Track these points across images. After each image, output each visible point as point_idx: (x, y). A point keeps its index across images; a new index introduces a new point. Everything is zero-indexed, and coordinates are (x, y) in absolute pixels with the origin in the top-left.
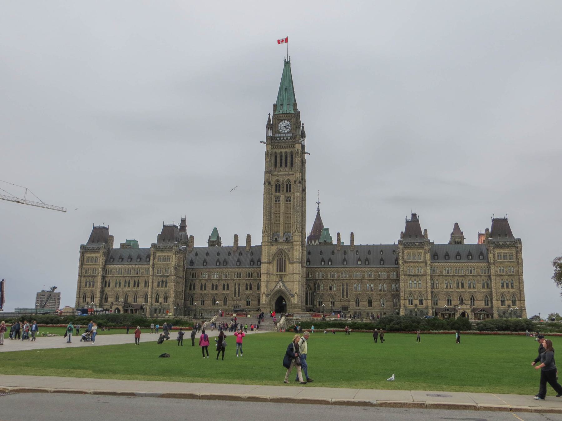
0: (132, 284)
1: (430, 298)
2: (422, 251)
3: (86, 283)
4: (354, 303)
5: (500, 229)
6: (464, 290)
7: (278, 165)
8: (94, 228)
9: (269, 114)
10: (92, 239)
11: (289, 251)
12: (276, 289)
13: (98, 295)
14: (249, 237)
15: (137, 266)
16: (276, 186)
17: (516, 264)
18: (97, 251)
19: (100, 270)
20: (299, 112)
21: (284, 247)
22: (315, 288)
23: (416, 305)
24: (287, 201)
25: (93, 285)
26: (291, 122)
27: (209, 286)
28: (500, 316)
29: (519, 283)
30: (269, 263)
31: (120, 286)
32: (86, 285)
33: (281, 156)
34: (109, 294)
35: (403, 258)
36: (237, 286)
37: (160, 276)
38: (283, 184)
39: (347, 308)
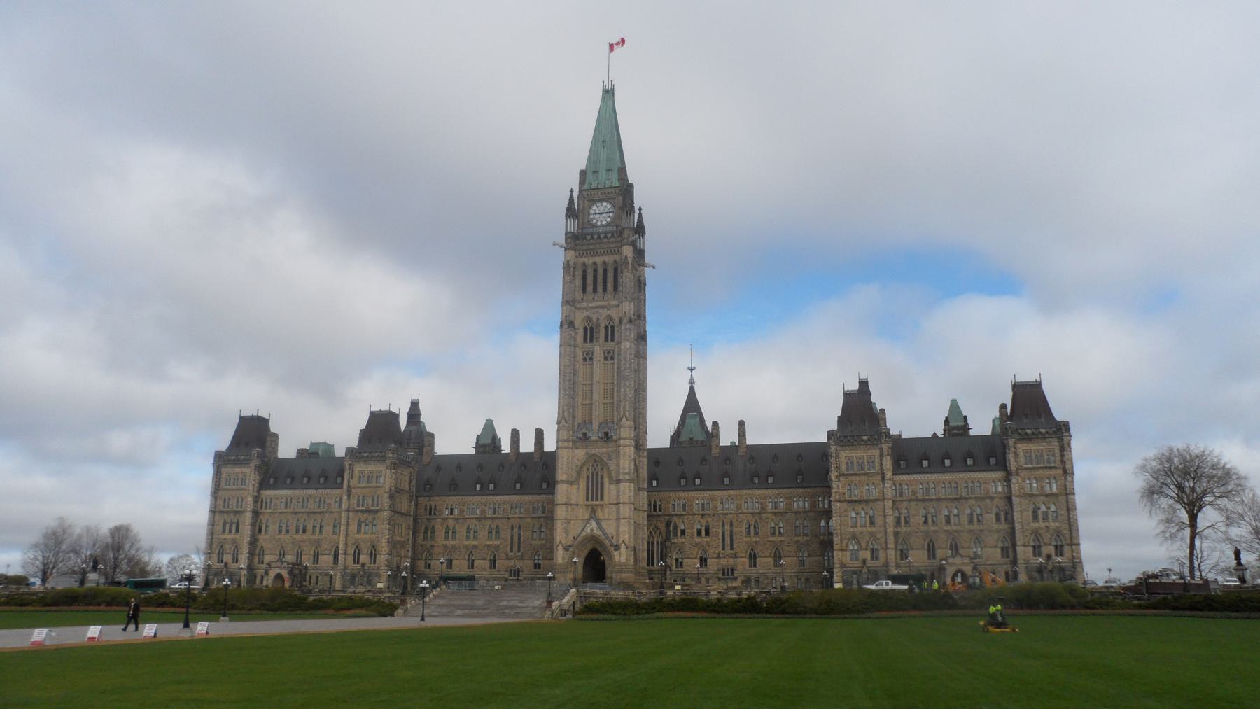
0: (309, 528)
1: (891, 545)
2: (875, 452)
3: (224, 526)
4: (747, 561)
5: (1029, 405)
6: (959, 528)
7: (590, 288)
8: (242, 418)
9: (572, 191)
11: (610, 458)
12: (584, 534)
13: (245, 549)
14: (539, 434)
15: (320, 492)
16: (585, 329)
17: (1060, 471)
18: (246, 463)
19: (250, 499)
20: (631, 186)
21: (601, 450)
22: (668, 532)
23: (864, 561)
24: (606, 359)
25: (237, 531)
26: (613, 206)
27: (462, 531)
28: (1031, 578)
29: (1068, 510)
30: (571, 483)
31: (287, 532)
32: (224, 531)
33: (595, 271)
35: (838, 468)
36: (516, 530)
38: (598, 325)
39: (732, 570)
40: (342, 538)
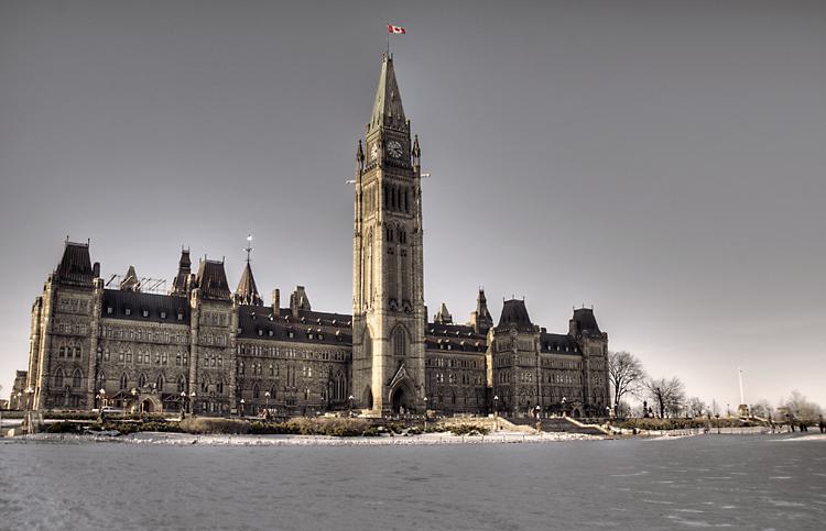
5: (584, 321)
15: (163, 325)
17: (602, 359)
19: (94, 324)
33: (393, 190)
36: (291, 369)
40: (192, 369)
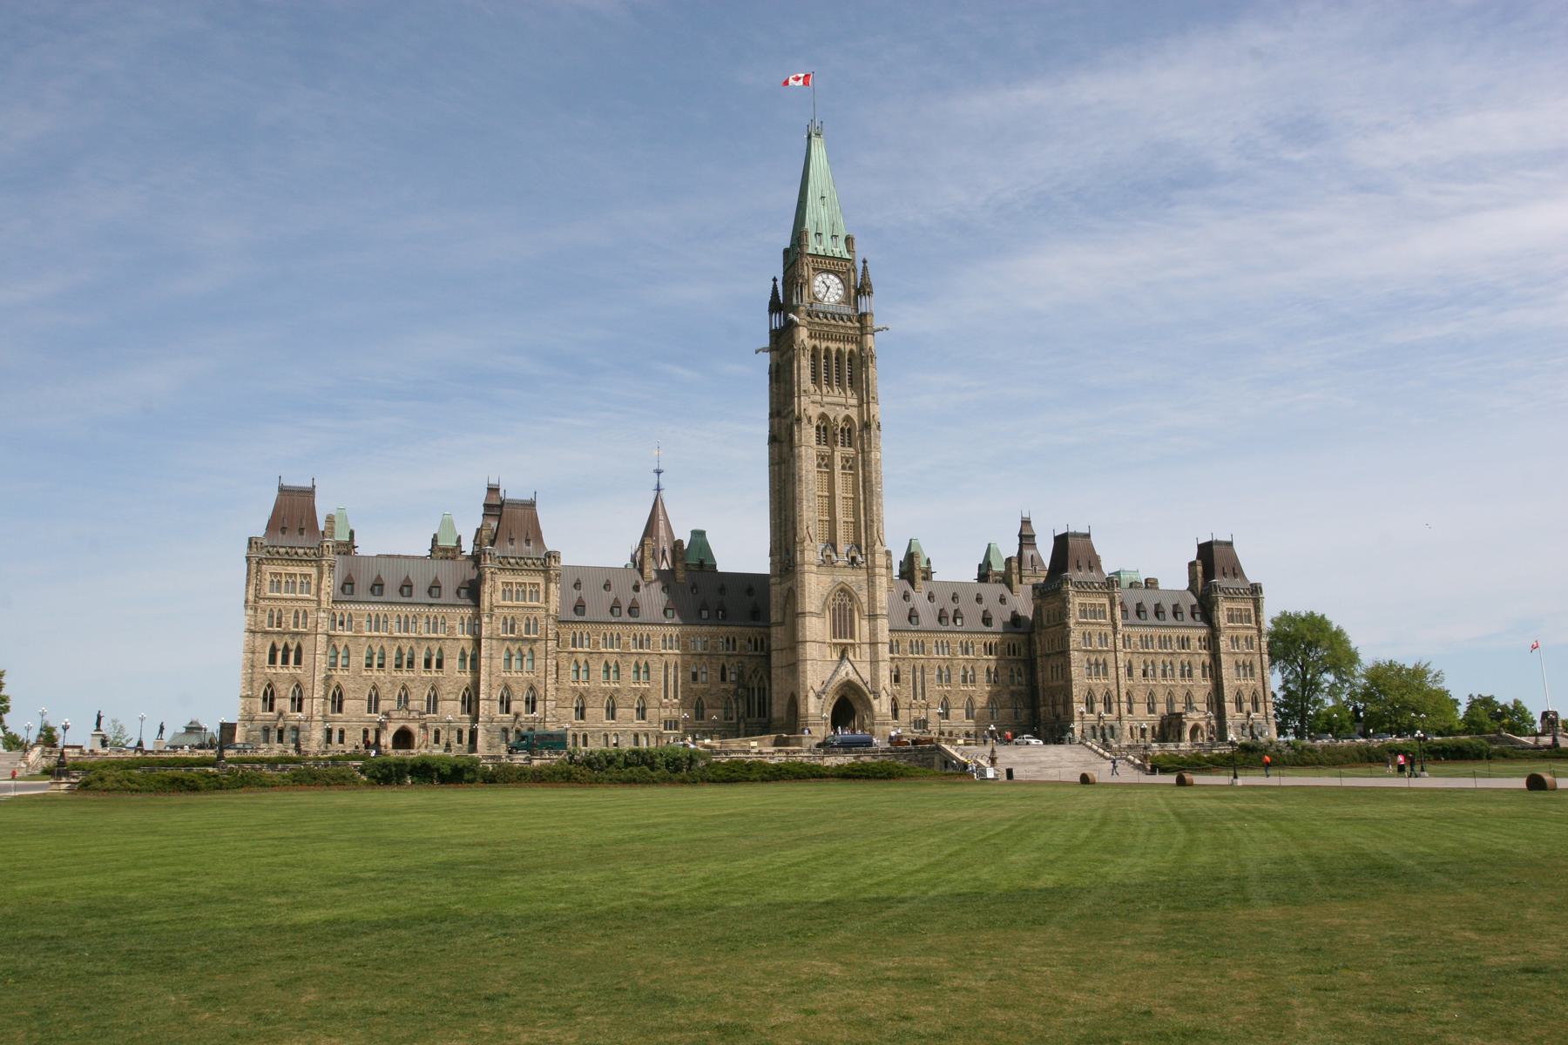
10: (277, 524)
11: (860, 588)
12: (838, 678)
13: (319, 691)
25: (298, 661)
31: (381, 666)
34: (348, 686)
37: (511, 639)
